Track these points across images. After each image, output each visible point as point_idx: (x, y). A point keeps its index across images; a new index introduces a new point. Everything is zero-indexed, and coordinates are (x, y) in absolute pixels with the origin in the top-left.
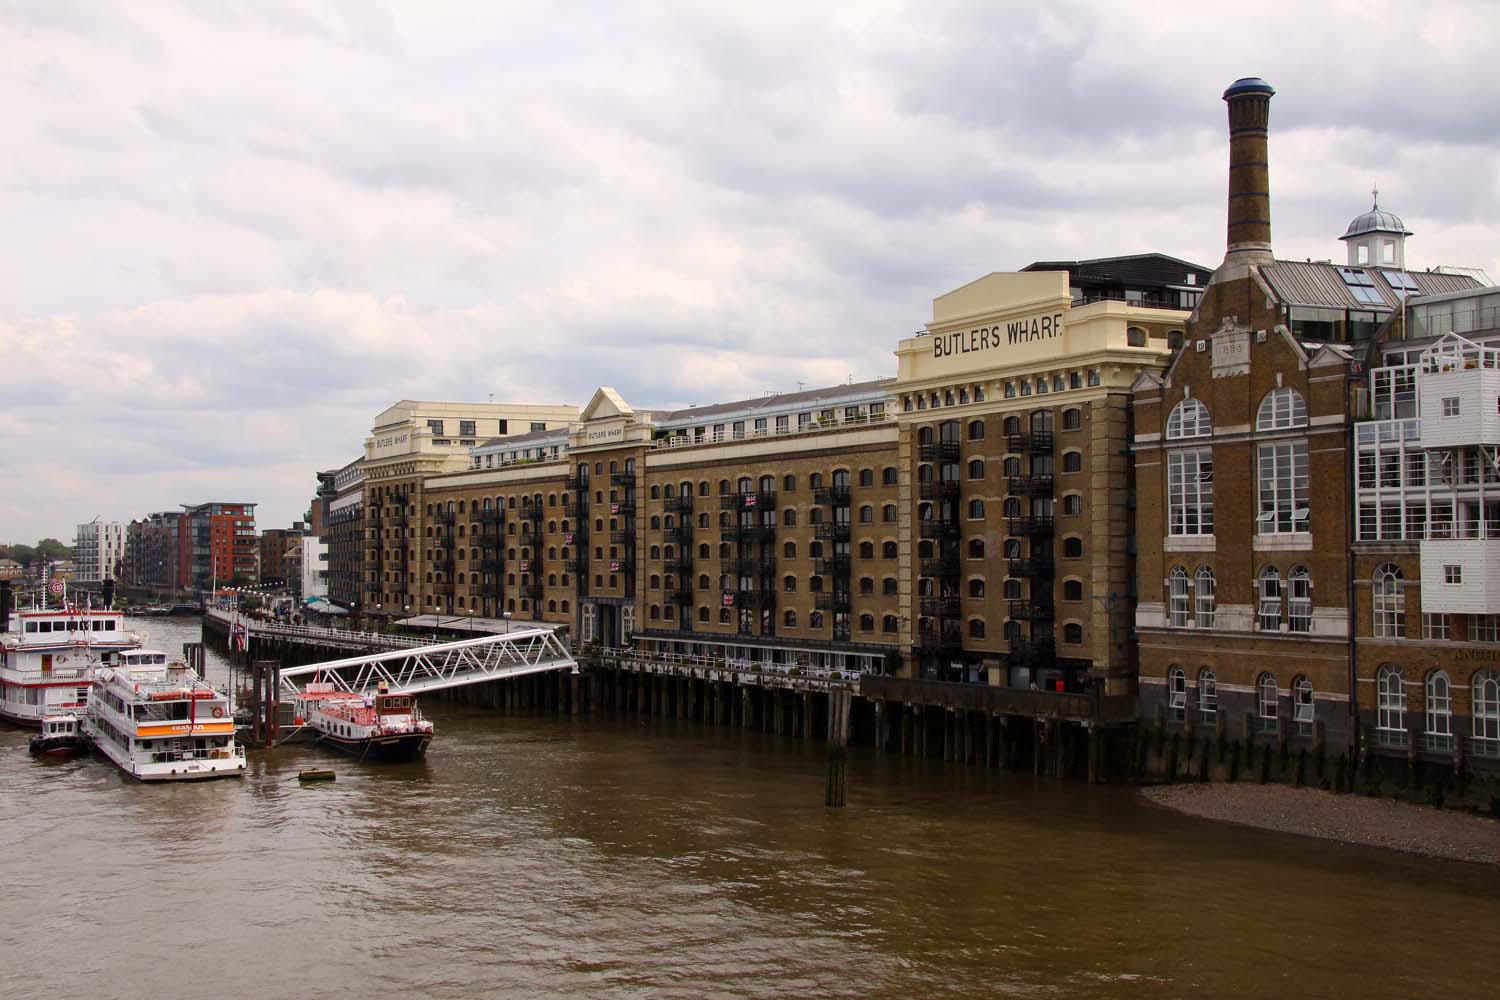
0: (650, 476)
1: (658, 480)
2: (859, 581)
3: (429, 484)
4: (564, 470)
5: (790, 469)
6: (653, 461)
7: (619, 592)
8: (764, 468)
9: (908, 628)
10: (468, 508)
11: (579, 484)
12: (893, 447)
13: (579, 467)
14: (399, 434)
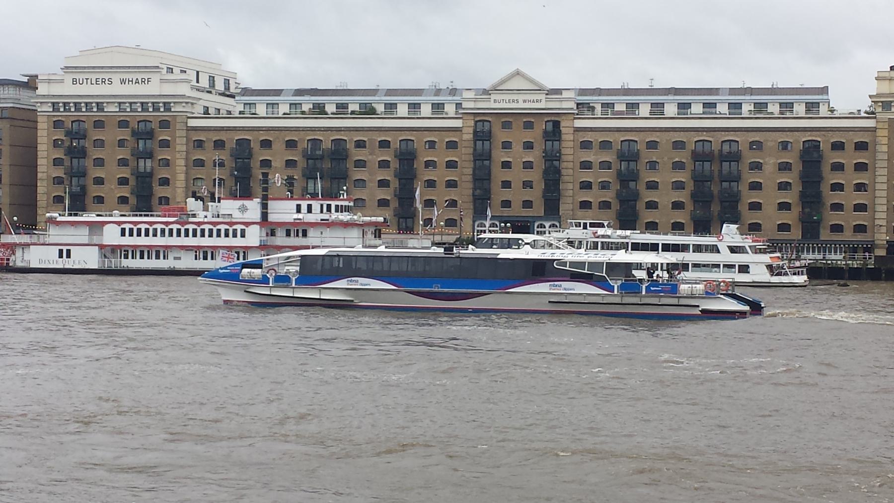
0: (580, 133)
1: (589, 137)
2: (829, 205)
3: (192, 123)
4: (458, 123)
5: (757, 137)
6: (579, 124)
7: (539, 209)
8: (726, 136)
9: (884, 229)
10: (278, 146)
11: (482, 135)
12: (873, 130)
13: (476, 122)
14: (146, 76)
